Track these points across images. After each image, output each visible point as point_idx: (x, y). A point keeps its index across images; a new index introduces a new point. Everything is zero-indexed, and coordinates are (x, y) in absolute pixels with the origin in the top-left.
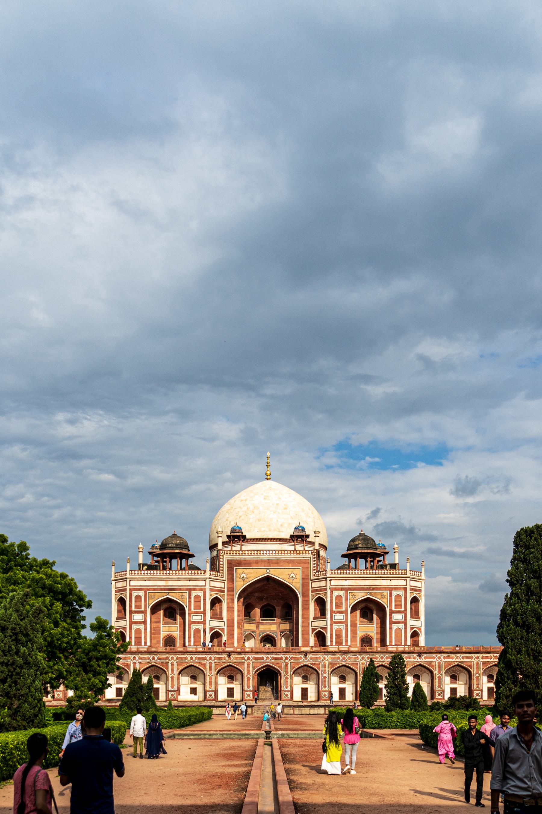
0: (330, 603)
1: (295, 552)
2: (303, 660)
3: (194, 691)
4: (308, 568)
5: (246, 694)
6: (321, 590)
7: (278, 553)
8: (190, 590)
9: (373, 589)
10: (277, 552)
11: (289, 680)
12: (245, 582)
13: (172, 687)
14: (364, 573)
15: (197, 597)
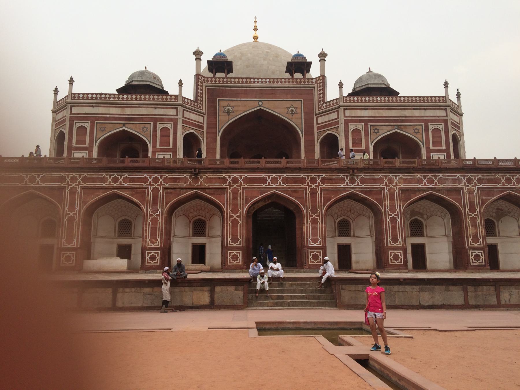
0: (345, 139)
1: (295, 80)
2: (347, 184)
3: (124, 252)
4: (312, 100)
5: (230, 253)
6: (330, 125)
7: (274, 82)
8: (155, 120)
9: (403, 121)
10: (272, 80)
11: (319, 226)
12: (230, 117)
13: (69, 240)
14: (389, 100)
15: (165, 130)
